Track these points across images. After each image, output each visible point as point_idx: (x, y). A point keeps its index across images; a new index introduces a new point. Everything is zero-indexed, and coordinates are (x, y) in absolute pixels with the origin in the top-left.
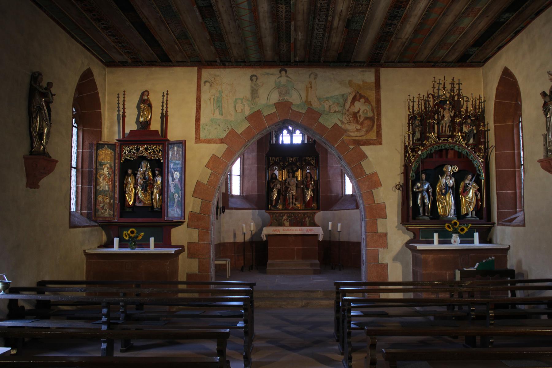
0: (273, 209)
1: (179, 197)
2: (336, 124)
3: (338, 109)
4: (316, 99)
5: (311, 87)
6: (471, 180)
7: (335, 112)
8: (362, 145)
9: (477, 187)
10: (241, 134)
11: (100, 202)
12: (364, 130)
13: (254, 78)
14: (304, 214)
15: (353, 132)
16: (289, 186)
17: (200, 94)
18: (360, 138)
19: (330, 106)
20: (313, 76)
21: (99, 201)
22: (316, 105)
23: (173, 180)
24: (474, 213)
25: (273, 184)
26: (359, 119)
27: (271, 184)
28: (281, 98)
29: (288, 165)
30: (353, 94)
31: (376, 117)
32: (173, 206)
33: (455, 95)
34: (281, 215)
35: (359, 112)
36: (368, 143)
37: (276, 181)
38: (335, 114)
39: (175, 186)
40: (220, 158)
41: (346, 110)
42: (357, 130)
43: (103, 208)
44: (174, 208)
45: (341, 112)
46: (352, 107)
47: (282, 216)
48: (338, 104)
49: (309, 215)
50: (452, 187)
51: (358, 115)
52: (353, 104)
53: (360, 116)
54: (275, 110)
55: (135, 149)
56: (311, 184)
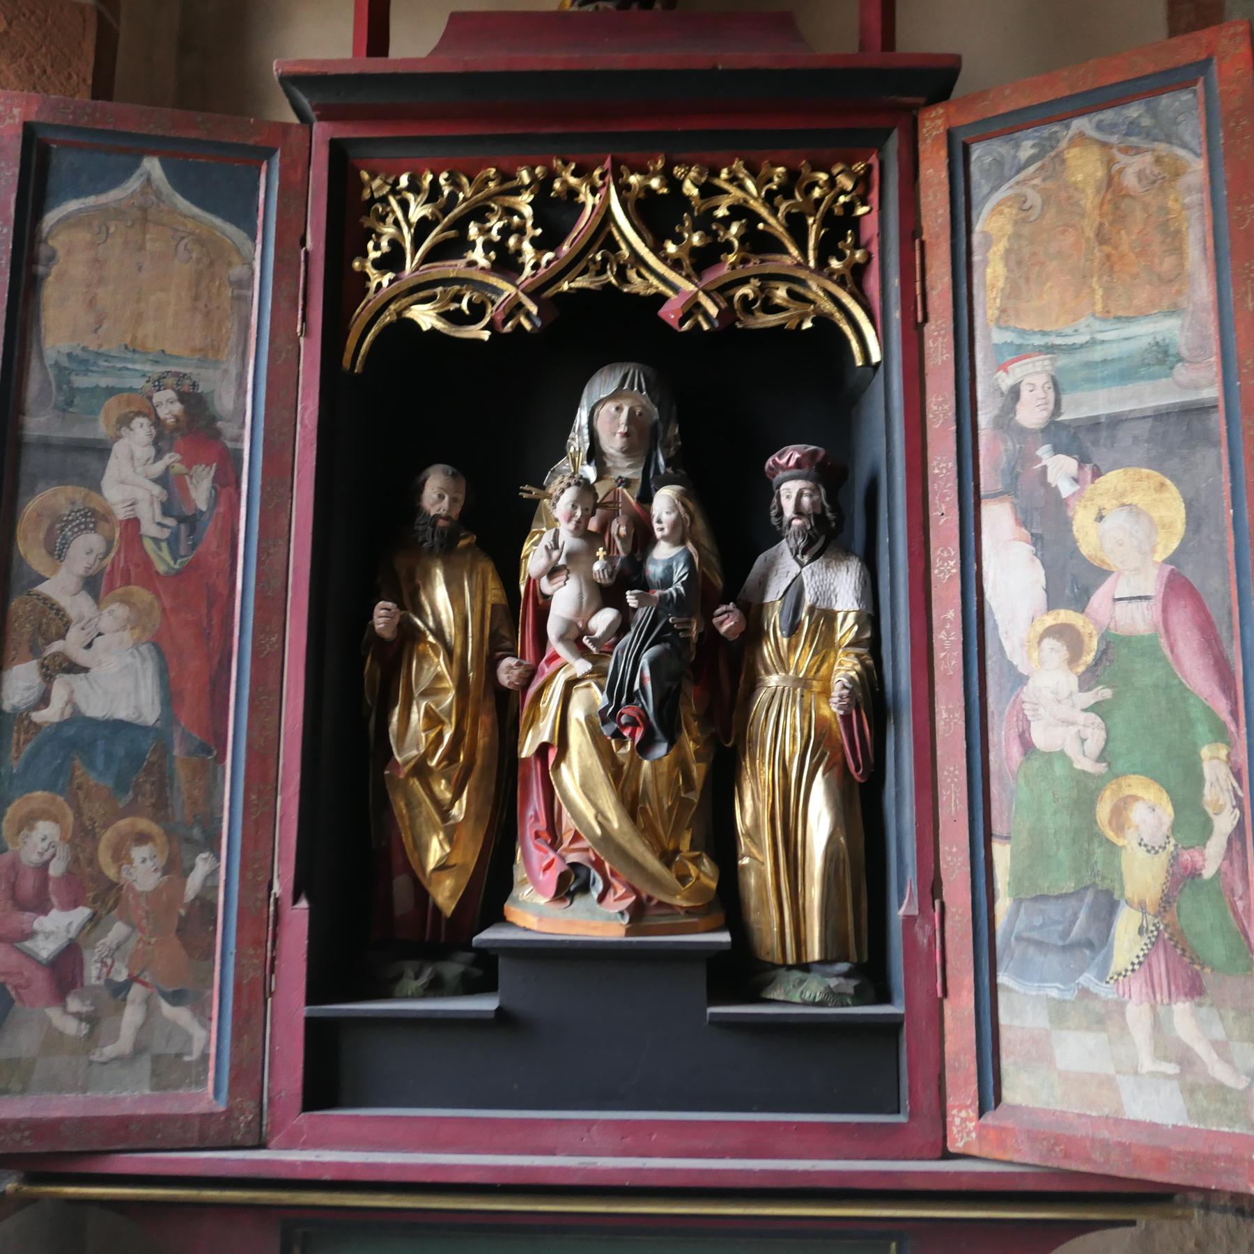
11: (28, 885)
44: (1105, 991)
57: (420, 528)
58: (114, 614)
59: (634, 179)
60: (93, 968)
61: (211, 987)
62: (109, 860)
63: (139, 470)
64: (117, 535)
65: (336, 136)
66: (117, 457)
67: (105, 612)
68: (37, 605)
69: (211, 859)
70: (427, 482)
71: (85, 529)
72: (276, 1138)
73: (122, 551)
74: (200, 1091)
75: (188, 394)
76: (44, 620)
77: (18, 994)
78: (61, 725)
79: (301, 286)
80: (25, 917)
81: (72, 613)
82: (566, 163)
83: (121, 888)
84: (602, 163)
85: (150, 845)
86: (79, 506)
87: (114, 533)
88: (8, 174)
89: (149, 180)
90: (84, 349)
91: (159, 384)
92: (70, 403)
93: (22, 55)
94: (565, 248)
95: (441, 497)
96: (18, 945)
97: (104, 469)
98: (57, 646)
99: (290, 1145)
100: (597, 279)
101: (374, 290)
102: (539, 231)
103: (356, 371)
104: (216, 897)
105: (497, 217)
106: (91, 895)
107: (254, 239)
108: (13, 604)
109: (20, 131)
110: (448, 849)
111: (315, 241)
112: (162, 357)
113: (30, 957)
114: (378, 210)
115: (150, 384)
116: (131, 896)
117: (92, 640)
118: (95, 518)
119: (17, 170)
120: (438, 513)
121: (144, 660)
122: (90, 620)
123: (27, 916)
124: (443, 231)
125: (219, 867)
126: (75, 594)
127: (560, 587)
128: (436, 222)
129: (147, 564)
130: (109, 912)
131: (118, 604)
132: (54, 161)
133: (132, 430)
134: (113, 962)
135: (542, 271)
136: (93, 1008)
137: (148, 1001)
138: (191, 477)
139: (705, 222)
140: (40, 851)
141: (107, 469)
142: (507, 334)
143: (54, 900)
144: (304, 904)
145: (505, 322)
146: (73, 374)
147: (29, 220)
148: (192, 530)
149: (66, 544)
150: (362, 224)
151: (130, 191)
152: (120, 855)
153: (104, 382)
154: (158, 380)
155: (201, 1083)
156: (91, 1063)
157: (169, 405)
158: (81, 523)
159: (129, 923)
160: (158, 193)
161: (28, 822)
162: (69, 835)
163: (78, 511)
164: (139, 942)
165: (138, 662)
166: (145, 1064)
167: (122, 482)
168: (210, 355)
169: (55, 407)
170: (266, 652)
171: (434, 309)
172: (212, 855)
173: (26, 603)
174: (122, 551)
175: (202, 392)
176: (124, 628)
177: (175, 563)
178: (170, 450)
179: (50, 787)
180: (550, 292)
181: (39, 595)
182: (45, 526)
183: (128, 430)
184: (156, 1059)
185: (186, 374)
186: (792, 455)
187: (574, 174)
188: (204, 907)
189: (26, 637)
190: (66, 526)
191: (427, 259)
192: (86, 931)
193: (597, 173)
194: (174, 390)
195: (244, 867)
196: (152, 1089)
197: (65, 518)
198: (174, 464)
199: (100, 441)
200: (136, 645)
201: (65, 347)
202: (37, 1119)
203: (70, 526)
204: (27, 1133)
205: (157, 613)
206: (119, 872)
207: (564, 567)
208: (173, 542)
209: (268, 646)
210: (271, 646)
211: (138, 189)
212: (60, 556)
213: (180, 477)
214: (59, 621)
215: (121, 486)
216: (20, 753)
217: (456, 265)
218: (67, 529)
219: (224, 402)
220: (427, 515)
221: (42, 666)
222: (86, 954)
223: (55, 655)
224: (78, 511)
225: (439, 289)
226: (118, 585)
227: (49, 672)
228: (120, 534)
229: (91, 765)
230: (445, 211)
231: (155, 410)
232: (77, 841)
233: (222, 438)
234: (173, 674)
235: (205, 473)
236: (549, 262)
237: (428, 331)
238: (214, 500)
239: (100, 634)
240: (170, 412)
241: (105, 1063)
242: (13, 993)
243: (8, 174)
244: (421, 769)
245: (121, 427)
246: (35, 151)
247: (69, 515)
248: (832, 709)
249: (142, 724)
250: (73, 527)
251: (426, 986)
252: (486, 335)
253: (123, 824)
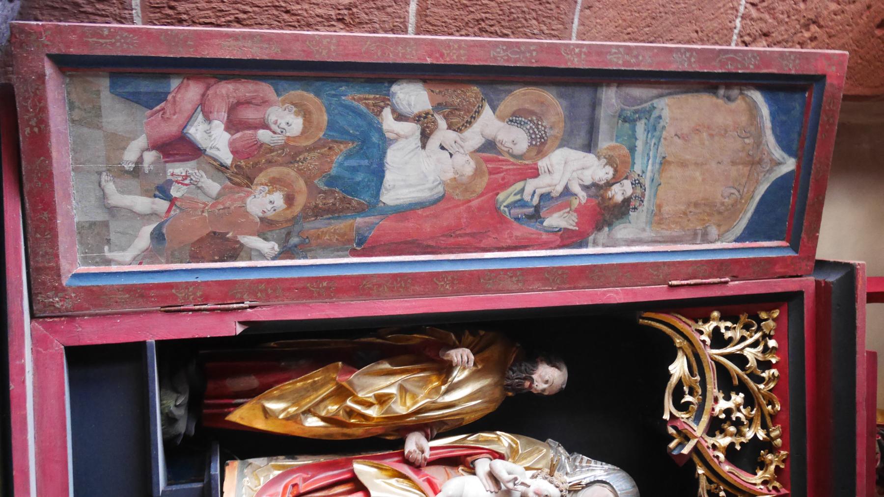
11: (250, 114)
21: (265, 103)
57: (523, 368)
58: (466, 165)
60: (181, 169)
61: (167, 262)
62: (272, 175)
63: (575, 175)
64: (526, 162)
65: (805, 296)
66: (584, 157)
67: (468, 157)
68: (474, 106)
69: (274, 253)
70: (557, 370)
71: (532, 138)
72: (40, 327)
73: (515, 167)
74: (78, 261)
75: (629, 205)
76: (462, 113)
77: (159, 111)
78: (380, 131)
79: (704, 281)
80: (223, 113)
81: (468, 133)
82: (784, 461)
83: (248, 187)
84: (784, 486)
85: (285, 206)
86: (550, 132)
87: (528, 160)
88: (791, 66)
89: (779, 164)
90: (664, 127)
92: (625, 120)
93: (857, 46)
94: (727, 468)
95: (546, 382)
96: (199, 109)
97: (576, 149)
98: (442, 123)
99: (39, 341)
100: (705, 492)
101: (698, 328)
102: (738, 448)
103: (641, 320)
104: (242, 260)
105: (747, 415)
106: (243, 163)
107: (736, 241)
108: (475, 88)
109: (819, 73)
110: (281, 416)
111: (735, 287)
112: (657, 185)
113: (190, 119)
114: (753, 327)
115: (636, 177)
116: (242, 195)
117: (447, 150)
118: (540, 147)
119: (793, 72)
120: (535, 382)
121: (431, 189)
122: (462, 147)
123: (224, 115)
124: (738, 375)
125: (268, 260)
126: (482, 134)
127: (485, 487)
128: (743, 368)
129: (504, 186)
130: (229, 179)
131: (475, 167)
132: (797, 96)
133: (604, 167)
134: (186, 185)
135: (711, 453)
136: (147, 172)
137: (154, 214)
138: (568, 212)
140: (278, 123)
141: (576, 151)
142: (666, 429)
143: (238, 135)
144: (239, 330)
145: (675, 428)
146: (646, 121)
147: (760, 82)
148: (530, 217)
149: (520, 124)
150: (743, 314)
151: (773, 151)
152: (275, 183)
153: (639, 144)
154: (639, 183)
155: (86, 261)
156: (100, 174)
157: (622, 192)
158: (536, 134)
159: (220, 195)
160: (770, 171)
161: (305, 112)
162: (292, 144)
163: (545, 132)
164: (204, 203)
165: (429, 185)
166: (100, 216)
167: (566, 163)
168: (656, 218)
169: (622, 110)
170: (437, 282)
171: (685, 375)
172: (277, 253)
173: (475, 98)
174: (515, 167)
175: (630, 215)
176: (456, 172)
177: (505, 207)
178: (589, 196)
179: (331, 126)
180: (696, 459)
181: (481, 107)
182: (536, 108)
183: (604, 164)
184: (105, 224)
185: (643, 201)
187: (777, 467)
188: (234, 251)
189: (449, 100)
190: (534, 124)
191: (719, 366)
192: (212, 162)
193: (777, 484)
194: (632, 194)
195: (269, 281)
196: (78, 223)
197: (540, 123)
198: (578, 200)
199: (596, 145)
200: (443, 183)
201: (666, 113)
202: (49, 137)
203: (534, 127)
204: (36, 130)
205: (468, 196)
206: (262, 184)
207: (500, 488)
208: (521, 203)
209: (442, 283)
210: (442, 285)
211: (774, 157)
212: (511, 121)
213: (569, 205)
214: (462, 124)
215: (563, 162)
216: (358, 102)
217: (715, 388)
218: (531, 125)
219: (622, 231)
220: (533, 371)
221: (427, 114)
222: (193, 163)
223: (435, 122)
224: (545, 132)
225: (698, 378)
226: (489, 166)
227: (422, 119)
228: (527, 164)
229: (348, 156)
230: (752, 376)
231: (617, 183)
232: (287, 150)
233: (596, 232)
234: (420, 212)
235: (571, 222)
236: (717, 457)
237: (668, 371)
238: (552, 231)
239: (451, 155)
240: (616, 193)
241: (100, 185)
242: (158, 108)
243: (791, 66)
245: (606, 158)
246: (806, 83)
247: (542, 126)
249: (381, 192)
250: (533, 130)
251: (170, 415)
252: (666, 416)
253: (301, 184)
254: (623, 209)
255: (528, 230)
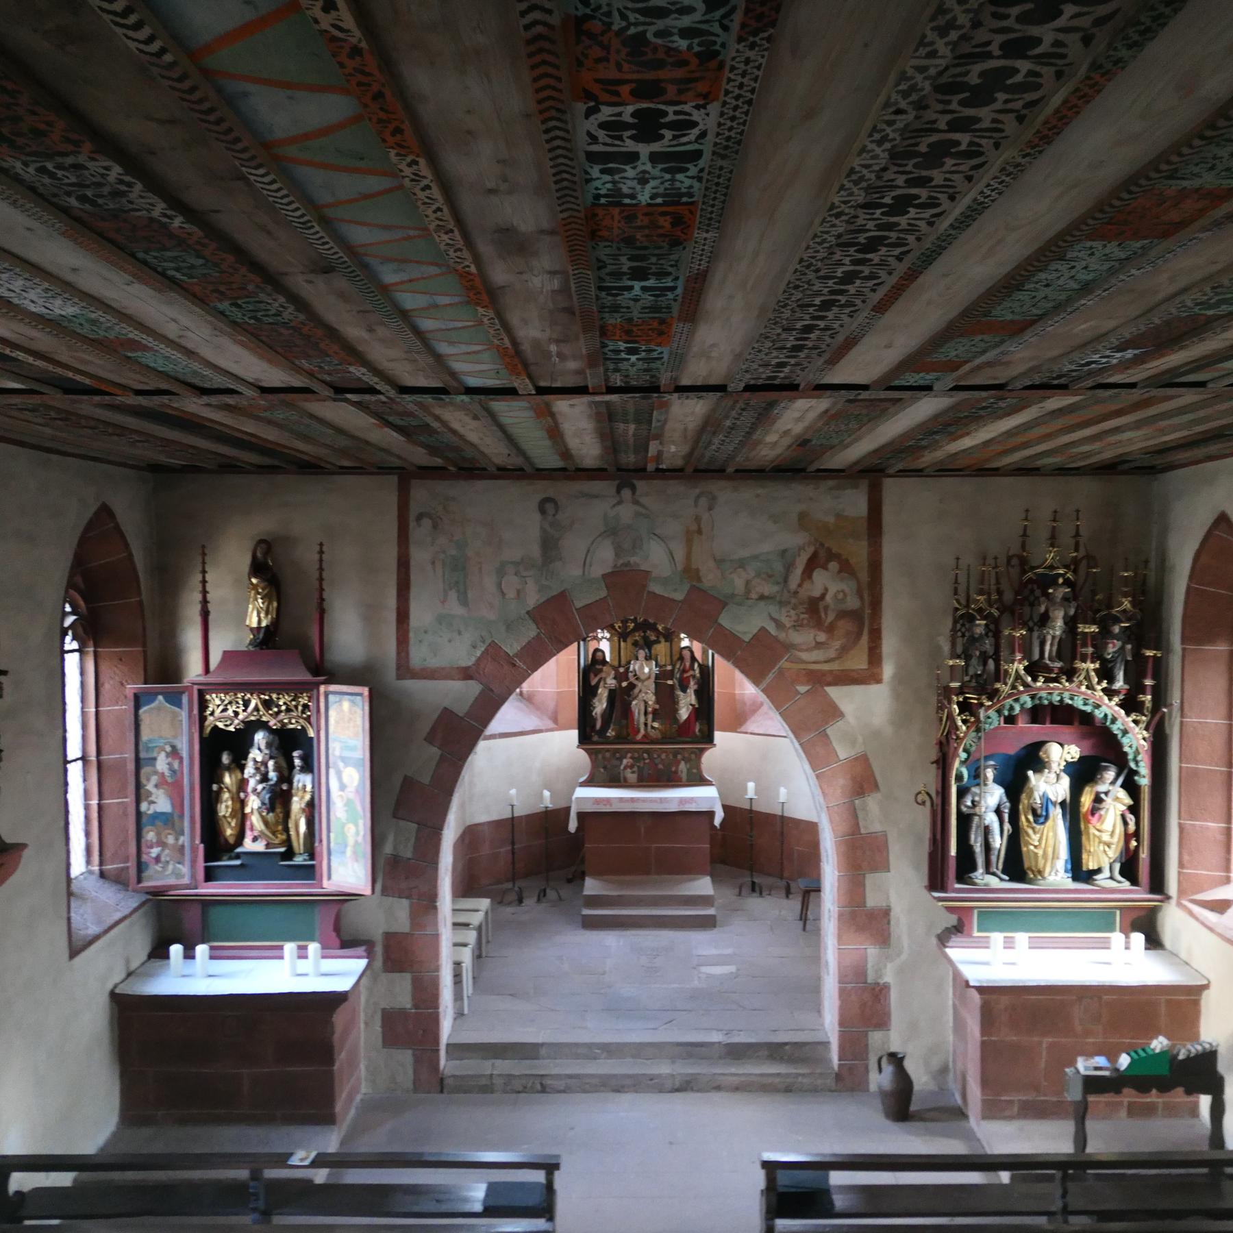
0: (595, 738)
1: (357, 833)
2: (763, 629)
3: (768, 589)
4: (711, 564)
5: (699, 532)
6: (1113, 783)
7: (762, 597)
8: (829, 684)
9: (1129, 801)
10: (516, 655)
12: (837, 644)
13: (550, 507)
14: (676, 753)
15: (807, 650)
16: (636, 682)
17: (407, 548)
18: (826, 667)
19: (748, 583)
20: (703, 501)
22: (710, 578)
23: (343, 787)
24: (1117, 866)
25: (596, 675)
26: (823, 615)
27: (592, 675)
28: (621, 562)
29: (634, 630)
30: (811, 550)
31: (868, 611)
32: (344, 853)
33: (1083, 558)
34: (618, 755)
35: (823, 597)
36: (847, 679)
37: (605, 668)
38: (762, 604)
39: (348, 803)
40: (461, 718)
41: (789, 592)
42: (819, 645)
43: (157, 859)
45: (778, 599)
46: (807, 585)
47: (620, 759)
48: (770, 576)
49: (686, 755)
50: (1063, 804)
51: (821, 605)
52: (810, 577)
53: (826, 608)
54: (603, 593)
55: (237, 703)
56: (694, 677)
59: (262, 696)
91: (166, 744)
111: (196, 711)
118: (156, 773)
139: (278, 706)
161: (148, 832)
186: (295, 754)
188: (183, 846)
219: (179, 746)
244: (224, 816)
248: (303, 805)
254: (173, 747)
255: (178, 773)
